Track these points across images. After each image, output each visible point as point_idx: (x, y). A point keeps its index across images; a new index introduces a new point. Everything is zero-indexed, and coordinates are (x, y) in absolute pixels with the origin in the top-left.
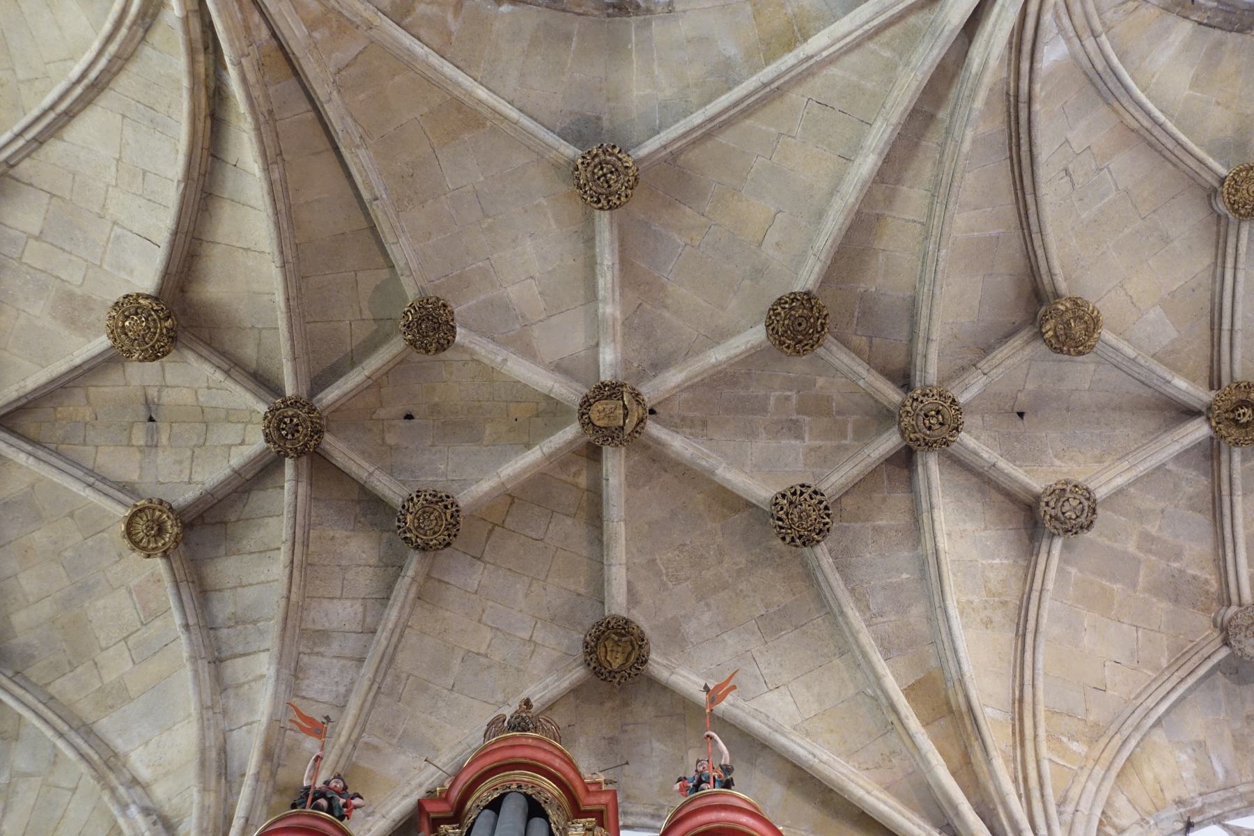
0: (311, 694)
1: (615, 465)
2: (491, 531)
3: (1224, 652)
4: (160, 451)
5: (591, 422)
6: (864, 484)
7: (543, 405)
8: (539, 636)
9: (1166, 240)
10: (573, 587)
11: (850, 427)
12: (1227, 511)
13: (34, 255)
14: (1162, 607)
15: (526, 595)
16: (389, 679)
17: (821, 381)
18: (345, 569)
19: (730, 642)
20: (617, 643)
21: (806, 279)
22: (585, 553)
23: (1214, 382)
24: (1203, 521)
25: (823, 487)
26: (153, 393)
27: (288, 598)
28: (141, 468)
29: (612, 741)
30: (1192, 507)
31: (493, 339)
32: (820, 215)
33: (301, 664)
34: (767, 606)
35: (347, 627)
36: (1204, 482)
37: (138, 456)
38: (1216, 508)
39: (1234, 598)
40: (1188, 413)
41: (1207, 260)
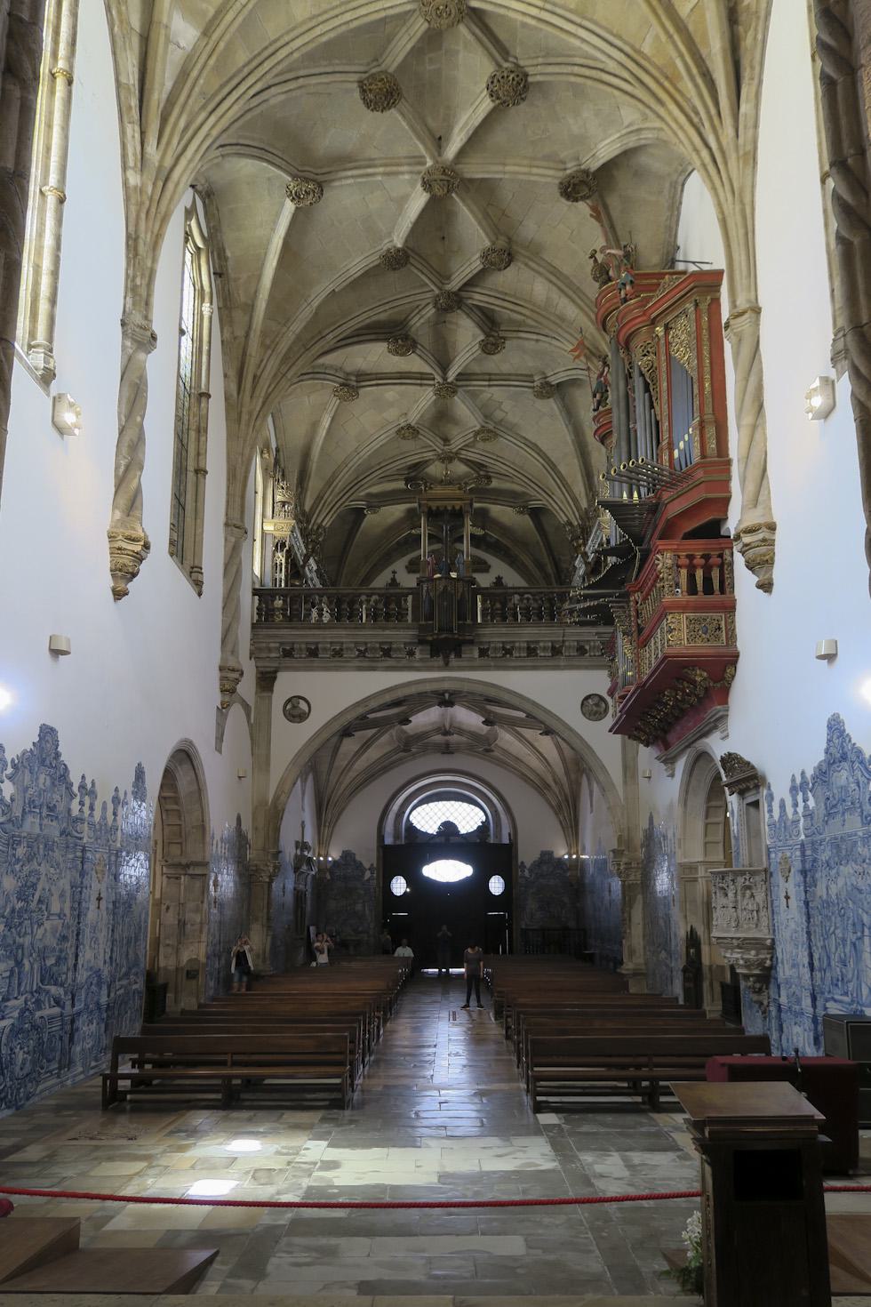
29: (636, 174)
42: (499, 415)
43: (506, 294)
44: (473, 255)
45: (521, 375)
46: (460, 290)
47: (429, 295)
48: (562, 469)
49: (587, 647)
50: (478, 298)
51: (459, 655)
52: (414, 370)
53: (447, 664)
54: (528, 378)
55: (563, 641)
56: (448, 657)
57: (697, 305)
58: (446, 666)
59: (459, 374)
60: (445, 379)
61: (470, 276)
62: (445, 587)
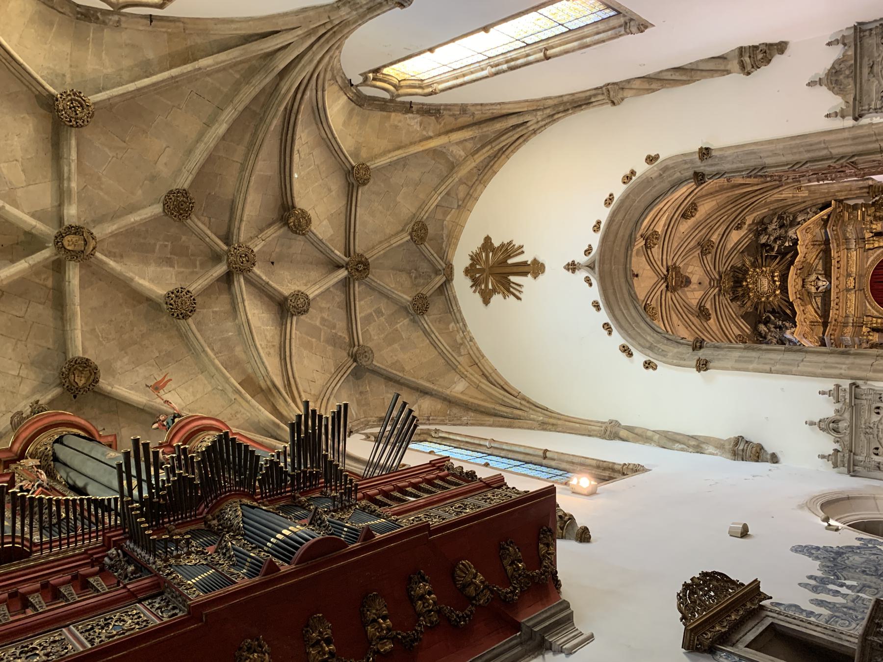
1: (74, 275)
3: (355, 364)
5: (63, 246)
6: (207, 291)
7: (22, 238)
9: (330, 190)
11: (198, 263)
12: (353, 308)
14: (330, 348)
15: (14, 350)
17: (184, 238)
19: (141, 371)
20: (81, 372)
21: (184, 182)
22: (52, 325)
23: (347, 253)
24: (342, 313)
25: (191, 290)
30: (339, 307)
32: (190, 152)
34: (160, 352)
36: (343, 296)
38: (349, 307)
39: (356, 343)
40: (339, 267)
41: (344, 202)
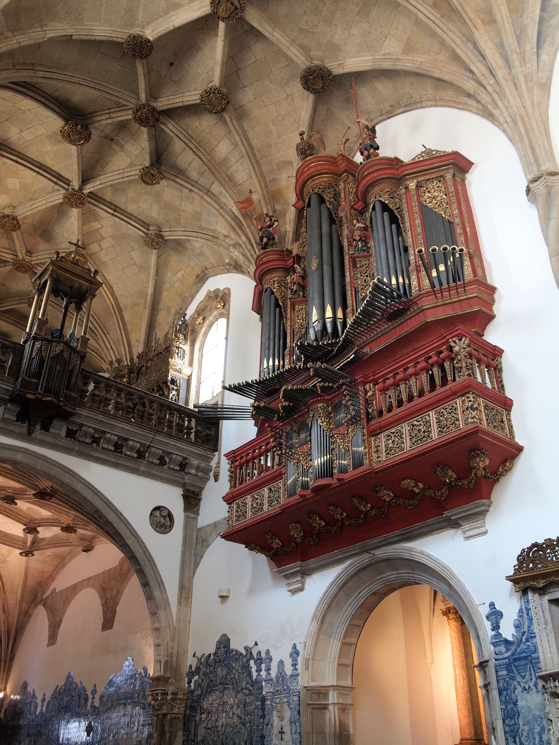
0: (241, 181)
2: (238, 75)
4: (125, 146)
8: (289, 91)
10: (283, 65)
13: (27, 136)
16: (257, 154)
18: (210, 133)
19: (355, 32)
26: (102, 134)
27: (205, 163)
28: (127, 156)
31: (162, 16)
33: (229, 175)
35: (230, 150)
37: (123, 153)
42: (94, 248)
43: (193, 138)
44: (195, 90)
45: (141, 220)
46: (163, 111)
47: (133, 101)
48: (127, 316)
49: (167, 460)
50: (170, 127)
51: (46, 428)
52: (53, 168)
53: (30, 433)
54: (147, 226)
55: (150, 446)
56: (34, 426)
57: (454, 176)
58: (28, 436)
59: (90, 192)
60: (81, 189)
61: (181, 104)
62: (62, 351)
